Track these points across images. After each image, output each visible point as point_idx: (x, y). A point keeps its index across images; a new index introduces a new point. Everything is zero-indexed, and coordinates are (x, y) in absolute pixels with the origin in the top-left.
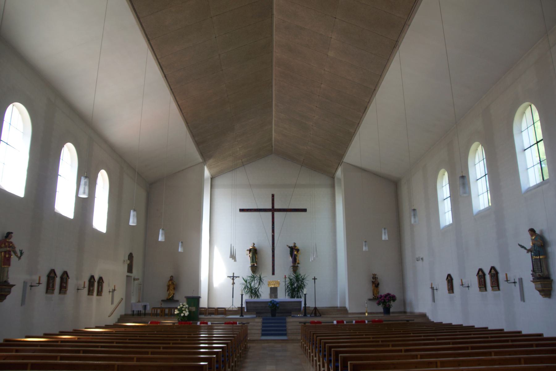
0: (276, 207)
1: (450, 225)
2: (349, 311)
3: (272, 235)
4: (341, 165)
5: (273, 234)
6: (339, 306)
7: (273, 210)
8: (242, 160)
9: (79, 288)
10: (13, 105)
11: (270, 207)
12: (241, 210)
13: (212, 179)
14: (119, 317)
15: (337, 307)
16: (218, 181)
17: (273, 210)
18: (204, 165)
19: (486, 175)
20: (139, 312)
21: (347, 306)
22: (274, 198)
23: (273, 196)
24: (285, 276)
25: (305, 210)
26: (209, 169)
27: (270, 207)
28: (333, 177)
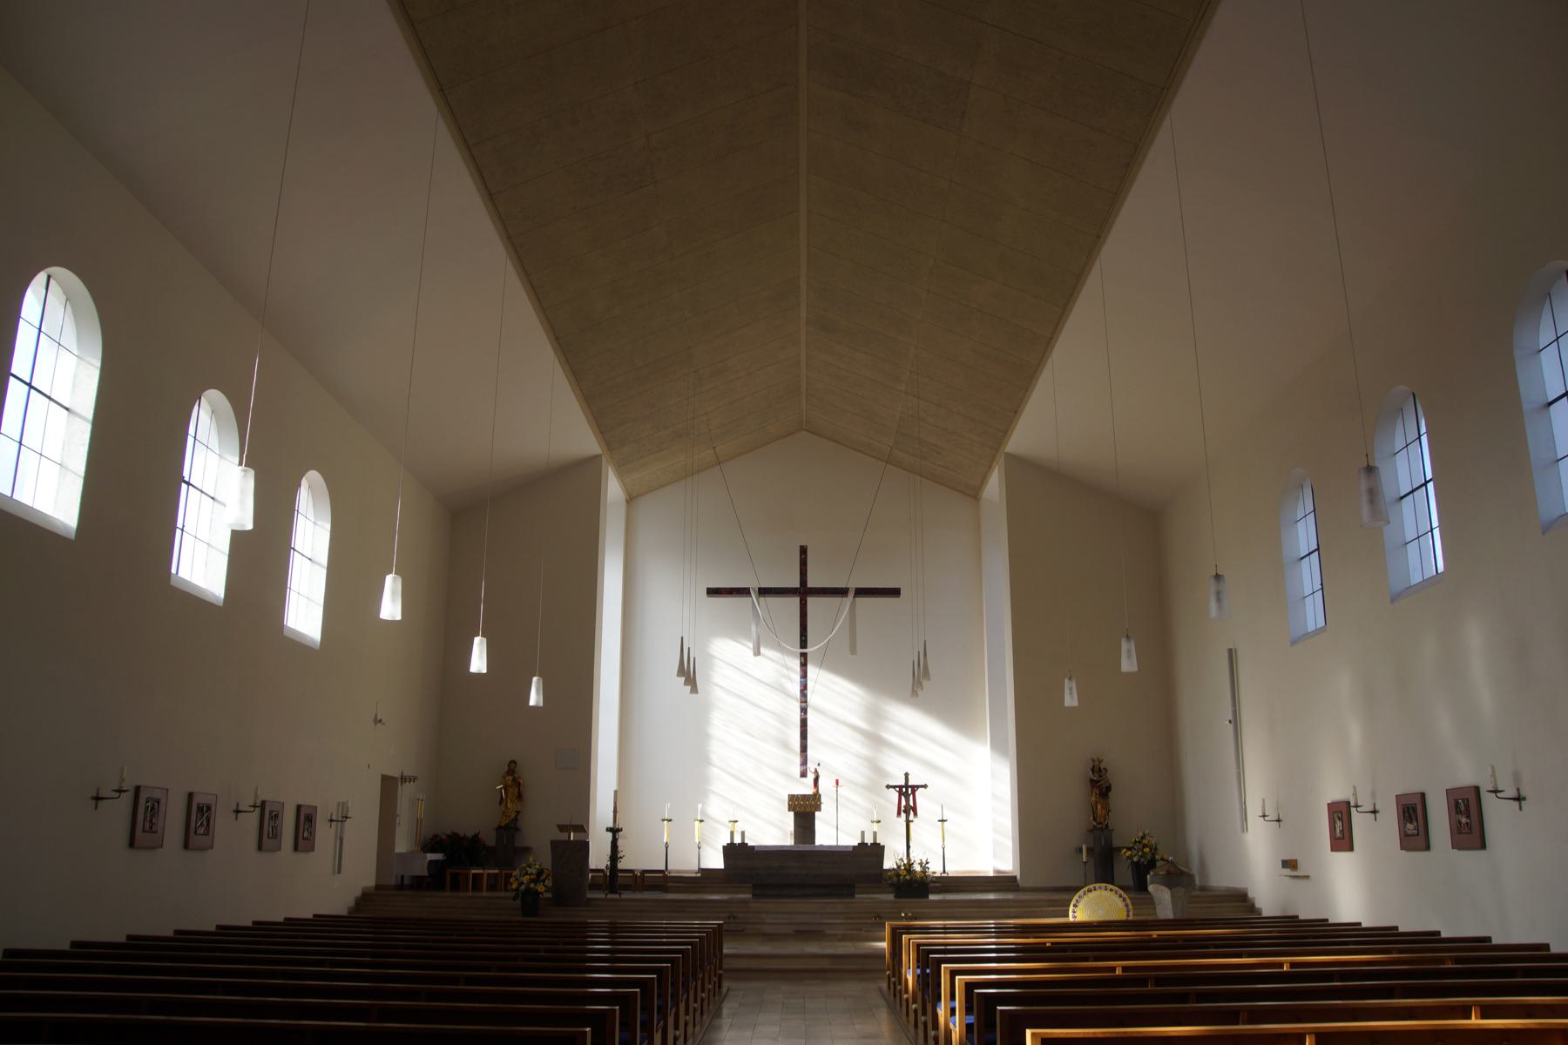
0: (810, 585)
1: (1318, 631)
2: (1021, 886)
5: (802, 659)
7: (804, 592)
8: (714, 448)
9: (240, 809)
10: (49, 277)
12: (712, 592)
13: (631, 499)
14: (358, 893)
19: (1427, 482)
22: (806, 558)
23: (803, 551)
25: (895, 592)
26: (621, 475)
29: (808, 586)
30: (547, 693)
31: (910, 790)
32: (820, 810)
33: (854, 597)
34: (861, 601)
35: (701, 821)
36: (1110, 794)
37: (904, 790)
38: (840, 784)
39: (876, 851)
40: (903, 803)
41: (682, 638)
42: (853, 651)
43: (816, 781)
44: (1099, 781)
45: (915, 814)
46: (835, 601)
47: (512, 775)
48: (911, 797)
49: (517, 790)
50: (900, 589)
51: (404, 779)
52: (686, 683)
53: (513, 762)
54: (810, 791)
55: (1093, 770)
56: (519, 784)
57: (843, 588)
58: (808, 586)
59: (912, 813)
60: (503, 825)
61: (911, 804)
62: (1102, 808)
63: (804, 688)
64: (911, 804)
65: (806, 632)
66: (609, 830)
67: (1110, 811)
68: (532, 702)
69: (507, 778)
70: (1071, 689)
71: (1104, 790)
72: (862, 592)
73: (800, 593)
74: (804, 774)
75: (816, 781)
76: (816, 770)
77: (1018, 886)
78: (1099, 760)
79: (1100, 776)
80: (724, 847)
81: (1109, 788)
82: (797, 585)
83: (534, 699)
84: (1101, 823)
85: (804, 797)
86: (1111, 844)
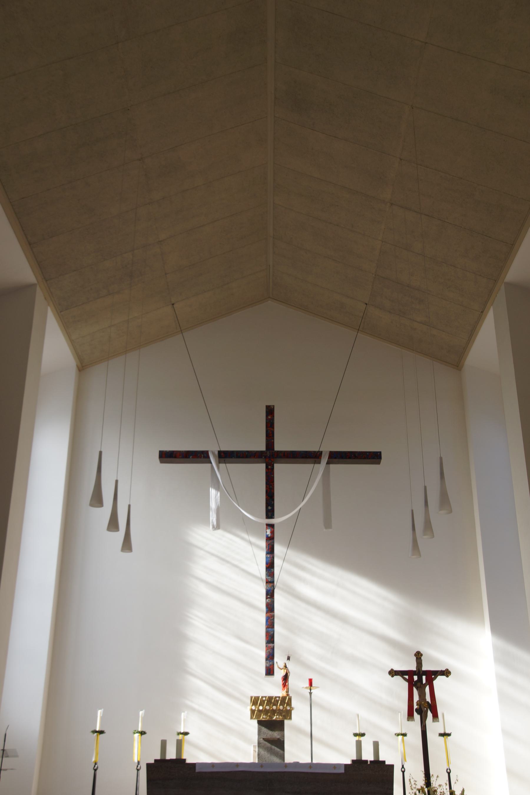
0: (278, 447)
23: (270, 411)
24: (311, 681)
31: (424, 677)
32: (290, 718)
33: (328, 463)
34: (338, 469)
35: (142, 733)
37: (416, 678)
38: (313, 685)
40: (416, 698)
42: (328, 524)
43: (286, 678)
45: (435, 716)
48: (427, 689)
50: (380, 452)
52: (113, 525)
54: (278, 692)
57: (315, 452)
59: (430, 714)
61: (428, 698)
63: (270, 566)
64: (428, 698)
73: (265, 457)
74: (270, 671)
82: (262, 447)
85: (270, 700)
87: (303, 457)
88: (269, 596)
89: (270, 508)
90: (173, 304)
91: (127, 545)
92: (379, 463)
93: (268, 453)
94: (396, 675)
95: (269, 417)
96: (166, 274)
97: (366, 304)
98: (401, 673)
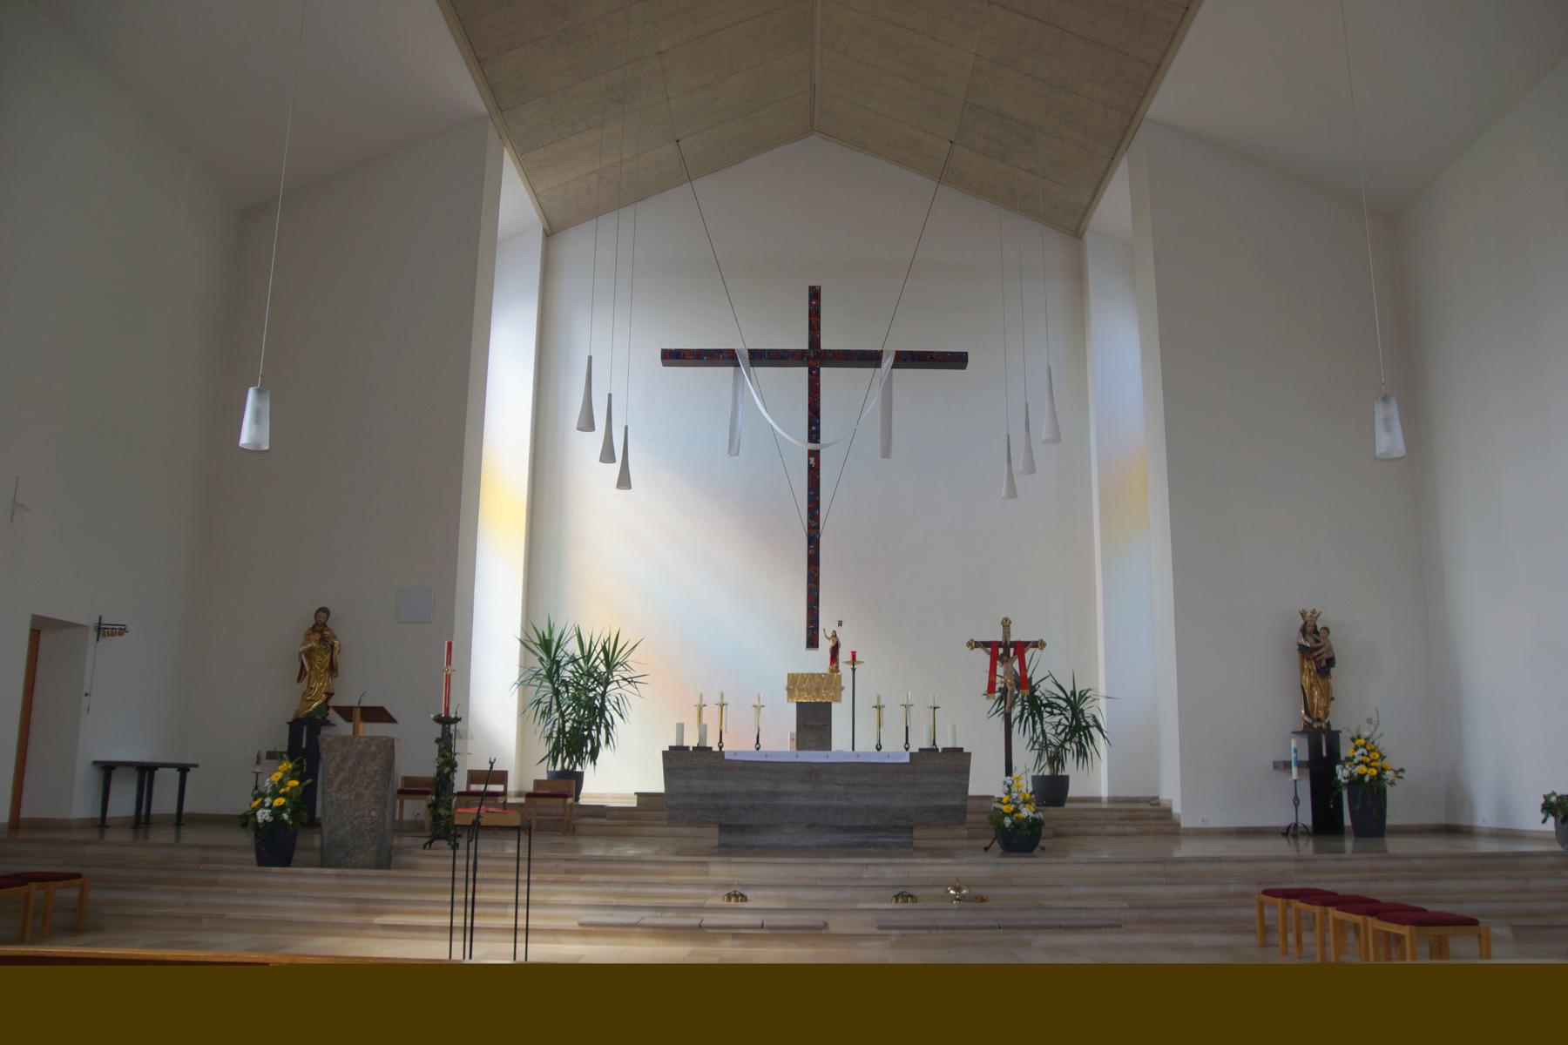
0: (826, 344)
2: (1185, 824)
3: (810, 466)
4: (1127, 149)
5: (812, 459)
6: (1104, 793)
11: (803, 345)
12: (672, 357)
13: (550, 234)
15: (1098, 800)
16: (577, 246)
17: (812, 354)
18: (504, 145)
20: (144, 811)
21: (1171, 792)
22: (818, 305)
23: (815, 294)
25: (957, 360)
26: (529, 175)
27: (803, 345)
28: (1077, 233)
29: (823, 347)
30: (279, 425)
31: (1012, 650)
33: (892, 368)
36: (1332, 670)
39: (957, 760)
41: (610, 396)
43: (835, 651)
44: (1317, 649)
46: (864, 373)
47: (321, 632)
49: (328, 657)
50: (966, 353)
51: (101, 630)
52: (608, 455)
53: (324, 610)
55: (1304, 631)
56: (332, 646)
57: (876, 351)
58: (823, 347)
60: (301, 716)
62: (1321, 695)
65: (819, 418)
66: (438, 719)
67: (1332, 699)
68: (245, 439)
69: (312, 637)
70: (1387, 420)
71: (1324, 664)
72: (907, 359)
73: (808, 358)
74: (812, 642)
75: (835, 651)
76: (835, 635)
77: (1178, 825)
78: (1313, 612)
79: (1317, 641)
80: (664, 753)
81: (1331, 662)
82: (806, 347)
83: (247, 435)
84: (1319, 720)
86: (1306, 762)
87: (859, 359)
88: (812, 547)
89: (814, 428)
90: (678, 141)
91: (624, 481)
92: (964, 368)
93: (812, 352)
94: (976, 647)
95: (814, 303)
96: (668, 98)
97: (951, 142)
98: (985, 645)
